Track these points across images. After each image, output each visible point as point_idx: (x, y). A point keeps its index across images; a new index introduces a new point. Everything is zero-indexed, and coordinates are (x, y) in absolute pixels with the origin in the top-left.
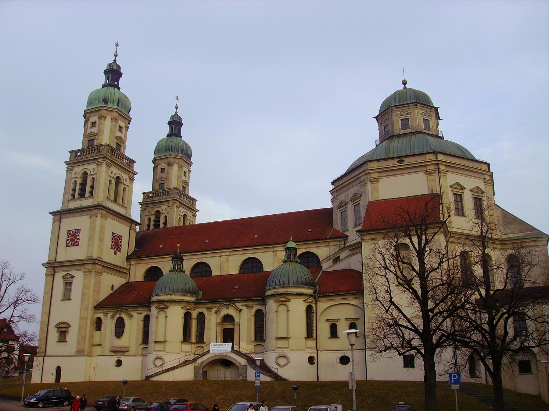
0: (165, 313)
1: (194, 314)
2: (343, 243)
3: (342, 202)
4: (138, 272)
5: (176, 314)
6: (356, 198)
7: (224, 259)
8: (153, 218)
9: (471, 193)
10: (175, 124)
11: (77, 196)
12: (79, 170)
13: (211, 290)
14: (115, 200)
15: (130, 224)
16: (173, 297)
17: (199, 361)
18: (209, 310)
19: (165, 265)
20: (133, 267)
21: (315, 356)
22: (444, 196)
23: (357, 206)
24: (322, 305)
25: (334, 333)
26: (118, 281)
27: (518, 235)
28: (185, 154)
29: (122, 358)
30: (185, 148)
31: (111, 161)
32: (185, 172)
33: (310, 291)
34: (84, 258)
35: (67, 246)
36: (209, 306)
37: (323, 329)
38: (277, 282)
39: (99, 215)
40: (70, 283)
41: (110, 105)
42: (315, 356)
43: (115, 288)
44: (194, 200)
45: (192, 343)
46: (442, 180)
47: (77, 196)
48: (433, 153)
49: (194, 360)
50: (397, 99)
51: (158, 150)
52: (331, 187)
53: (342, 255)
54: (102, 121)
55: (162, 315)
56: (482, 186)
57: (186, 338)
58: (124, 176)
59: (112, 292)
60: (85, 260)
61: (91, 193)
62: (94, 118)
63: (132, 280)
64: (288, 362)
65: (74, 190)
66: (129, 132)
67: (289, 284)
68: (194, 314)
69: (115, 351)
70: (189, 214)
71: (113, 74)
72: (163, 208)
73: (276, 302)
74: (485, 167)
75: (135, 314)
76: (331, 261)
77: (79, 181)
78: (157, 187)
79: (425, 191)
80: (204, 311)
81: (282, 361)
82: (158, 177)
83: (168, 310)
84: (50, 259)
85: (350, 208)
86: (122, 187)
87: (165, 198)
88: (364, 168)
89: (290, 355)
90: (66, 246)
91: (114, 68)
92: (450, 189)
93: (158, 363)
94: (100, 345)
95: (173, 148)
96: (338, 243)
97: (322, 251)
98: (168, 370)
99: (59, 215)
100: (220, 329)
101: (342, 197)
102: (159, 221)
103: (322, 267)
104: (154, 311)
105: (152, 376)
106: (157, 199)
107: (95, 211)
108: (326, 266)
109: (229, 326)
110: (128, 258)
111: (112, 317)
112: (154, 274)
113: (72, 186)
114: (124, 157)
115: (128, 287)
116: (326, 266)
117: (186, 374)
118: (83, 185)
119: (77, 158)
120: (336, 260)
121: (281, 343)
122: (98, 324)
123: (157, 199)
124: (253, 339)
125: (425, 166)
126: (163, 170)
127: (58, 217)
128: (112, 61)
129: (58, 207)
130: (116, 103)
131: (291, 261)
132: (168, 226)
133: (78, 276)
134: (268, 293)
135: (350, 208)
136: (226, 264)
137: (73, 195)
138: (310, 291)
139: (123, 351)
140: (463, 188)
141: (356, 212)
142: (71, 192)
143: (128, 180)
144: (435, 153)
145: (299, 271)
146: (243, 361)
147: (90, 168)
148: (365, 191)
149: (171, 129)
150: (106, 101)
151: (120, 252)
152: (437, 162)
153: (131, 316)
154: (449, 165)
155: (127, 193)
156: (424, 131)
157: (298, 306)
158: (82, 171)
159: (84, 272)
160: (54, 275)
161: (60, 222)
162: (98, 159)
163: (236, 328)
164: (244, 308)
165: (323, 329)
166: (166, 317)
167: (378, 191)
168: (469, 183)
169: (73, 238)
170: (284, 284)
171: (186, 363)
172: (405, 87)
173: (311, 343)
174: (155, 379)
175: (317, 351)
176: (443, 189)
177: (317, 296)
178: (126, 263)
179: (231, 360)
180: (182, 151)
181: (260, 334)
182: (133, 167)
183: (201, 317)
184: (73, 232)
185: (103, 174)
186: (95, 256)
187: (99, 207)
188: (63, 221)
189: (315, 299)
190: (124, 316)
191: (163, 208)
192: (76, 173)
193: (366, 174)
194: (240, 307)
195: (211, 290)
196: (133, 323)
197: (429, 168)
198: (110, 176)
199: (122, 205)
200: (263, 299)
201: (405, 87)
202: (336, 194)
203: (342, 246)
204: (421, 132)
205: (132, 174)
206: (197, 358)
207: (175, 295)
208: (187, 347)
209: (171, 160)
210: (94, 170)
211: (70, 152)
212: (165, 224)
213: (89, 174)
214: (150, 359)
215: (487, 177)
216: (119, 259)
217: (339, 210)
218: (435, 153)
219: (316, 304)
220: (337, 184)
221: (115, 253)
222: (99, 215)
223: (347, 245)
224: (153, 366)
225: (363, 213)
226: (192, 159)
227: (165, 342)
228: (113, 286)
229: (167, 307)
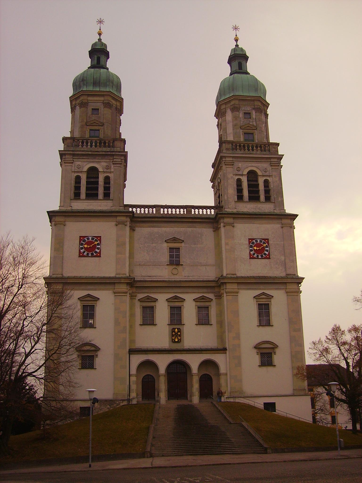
11: (83, 195)
34: (113, 275)
35: (81, 255)
47: (83, 195)
61: (107, 196)
65: (77, 188)
162: (113, 155)
169: (90, 247)
184: (88, 239)
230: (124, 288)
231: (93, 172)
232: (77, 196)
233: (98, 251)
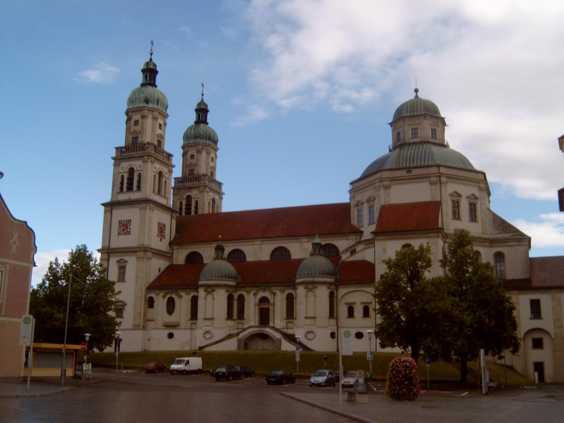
0: (213, 295)
1: (236, 296)
2: (359, 237)
3: (358, 202)
4: (180, 257)
5: (221, 296)
6: (370, 200)
7: (256, 247)
8: (184, 202)
9: (467, 200)
10: (202, 112)
12: (126, 166)
13: (249, 276)
14: (159, 193)
15: (170, 214)
16: (219, 282)
17: (241, 335)
18: (248, 292)
19: (207, 252)
20: (175, 252)
21: (336, 332)
22: (444, 204)
23: (371, 208)
24: (342, 291)
25: (351, 313)
26: (163, 264)
28: (211, 140)
29: (174, 331)
30: (212, 135)
31: (155, 158)
32: (212, 158)
33: (332, 280)
35: (119, 234)
36: (248, 289)
37: (343, 310)
38: (306, 272)
39: (148, 208)
40: (124, 267)
41: (150, 105)
42: (336, 332)
43: (162, 270)
44: (220, 184)
45: (234, 320)
46: (443, 190)
49: (238, 334)
50: (409, 109)
51: (186, 137)
52: (349, 187)
53: (358, 248)
54: (144, 120)
55: (209, 297)
56: (477, 193)
57: (230, 316)
58: (165, 170)
59: (159, 274)
60: (136, 248)
61: (139, 188)
62: (136, 117)
63: (175, 262)
64: (315, 337)
65: (122, 184)
66: (167, 128)
67: (315, 274)
68: (236, 296)
69: (167, 326)
70: (217, 197)
71: (150, 73)
72: (194, 193)
73: (305, 288)
74: (481, 177)
75: (183, 294)
76: (349, 253)
77: (126, 176)
78: (188, 173)
80: (244, 293)
81: (310, 336)
82: (188, 163)
83: (215, 293)
84: (105, 245)
85: (366, 207)
86: (164, 179)
87: (196, 183)
89: (317, 331)
90: (119, 234)
91: (152, 67)
93: (208, 336)
94: (153, 320)
95: (201, 136)
96: (354, 237)
97: (342, 244)
98: (217, 342)
99: (110, 206)
100: (257, 308)
101: (359, 197)
102: (191, 205)
103: (341, 258)
104: (202, 293)
105: (204, 347)
106: (188, 184)
107: (143, 205)
108: (345, 257)
109: (264, 306)
110: (171, 244)
111: (164, 297)
112: (194, 259)
113: (120, 180)
114: (163, 152)
115: (172, 268)
116: (345, 257)
117: (231, 346)
118: (131, 179)
119: (122, 155)
120: (353, 252)
121: (309, 321)
122: (150, 303)
123: (188, 184)
124: (285, 317)
126: (192, 157)
127: (109, 208)
128: (148, 60)
129: (108, 198)
130: (156, 103)
131: (317, 255)
132: (200, 212)
133: (132, 262)
134: (298, 281)
135: (366, 207)
136: (258, 252)
137: (122, 189)
138: (332, 280)
139: (175, 326)
140: (460, 196)
141: (371, 212)
142: (119, 186)
143: (168, 173)
145: (322, 262)
146: (278, 336)
147: (137, 164)
149: (198, 116)
150: (147, 101)
151: (164, 238)
152: (439, 174)
153: (181, 297)
154: (449, 177)
155: (167, 184)
156: (432, 140)
157: (323, 293)
158: (129, 167)
159: (137, 258)
160: (108, 260)
161: (111, 213)
162: (143, 157)
163: (271, 308)
164: (278, 292)
165: (343, 310)
166: (213, 298)
168: (466, 190)
169: (125, 227)
170: (311, 274)
171: (230, 336)
172: (417, 96)
173: (333, 322)
174: (207, 349)
175: (338, 328)
176: (444, 198)
177: (338, 284)
178: (169, 248)
179: (268, 334)
180: (210, 139)
181: (290, 313)
182: (171, 161)
183: (241, 299)
185: (149, 170)
186: (146, 244)
187: (147, 201)
188: (114, 212)
189: (336, 285)
190: (174, 296)
191: (194, 193)
192: (123, 168)
194: (275, 291)
195: (249, 276)
196: (183, 303)
198: (154, 172)
199: (165, 197)
200: (294, 286)
201: (417, 96)
202: (353, 194)
203: (358, 240)
204: (428, 142)
205: (170, 167)
206: (240, 332)
207: (220, 280)
208: (230, 323)
209: (200, 147)
210: (140, 166)
211: (117, 148)
212: (196, 208)
213: (135, 169)
214: (199, 333)
215: (482, 185)
216: (163, 245)
217: (356, 208)
218: (438, 166)
219: (337, 290)
221: (161, 240)
222: (148, 208)
223: (363, 239)
224: (203, 339)
225: (376, 214)
226: (219, 145)
227: (213, 319)
228: (160, 269)
229: (214, 291)
230: (141, 254)
231: (131, 171)
232: (122, 189)
233: (129, 230)
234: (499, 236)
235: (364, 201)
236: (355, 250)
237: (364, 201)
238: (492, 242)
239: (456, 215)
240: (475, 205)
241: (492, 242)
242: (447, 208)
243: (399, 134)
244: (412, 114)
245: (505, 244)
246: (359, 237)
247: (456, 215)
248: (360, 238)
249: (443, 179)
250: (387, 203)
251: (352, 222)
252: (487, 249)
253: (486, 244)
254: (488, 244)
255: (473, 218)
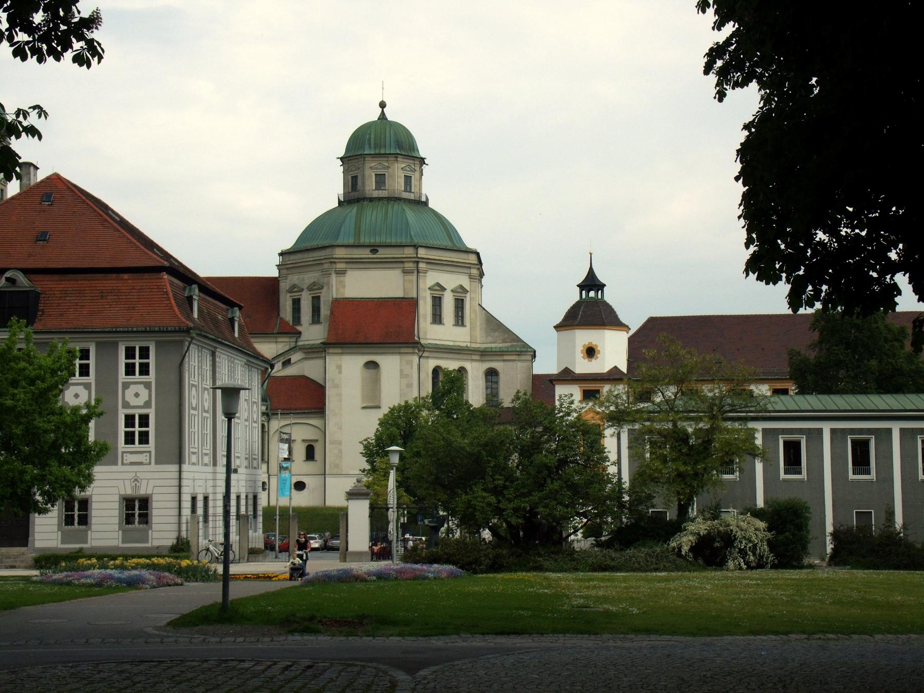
2: (294, 340)
9: (452, 294)
24: (275, 424)
27: (501, 345)
46: (421, 281)
48: (414, 246)
53: (295, 357)
79: (399, 294)
88: (327, 252)
92: (429, 292)
96: (287, 340)
120: (287, 363)
125: (403, 262)
140: (443, 289)
144: (416, 247)
148: (328, 284)
154: (430, 262)
156: (406, 195)
167: (344, 287)
172: (383, 116)
176: (421, 294)
193: (331, 262)
197: (406, 265)
201: (383, 116)
202: (285, 272)
203: (293, 345)
215: (474, 272)
217: (289, 295)
220: (287, 257)
223: (300, 343)
234: (493, 345)
235: (305, 287)
236: (290, 360)
237: (305, 287)
238: (484, 354)
239: (437, 318)
240: (462, 300)
241: (484, 354)
242: (425, 308)
243: (355, 178)
244: (377, 152)
245: (501, 358)
246: (294, 340)
247: (437, 318)
248: (296, 342)
249: (421, 265)
250: (339, 296)
251: (282, 315)
252: (475, 364)
253: (474, 357)
254: (477, 357)
255: (459, 320)
